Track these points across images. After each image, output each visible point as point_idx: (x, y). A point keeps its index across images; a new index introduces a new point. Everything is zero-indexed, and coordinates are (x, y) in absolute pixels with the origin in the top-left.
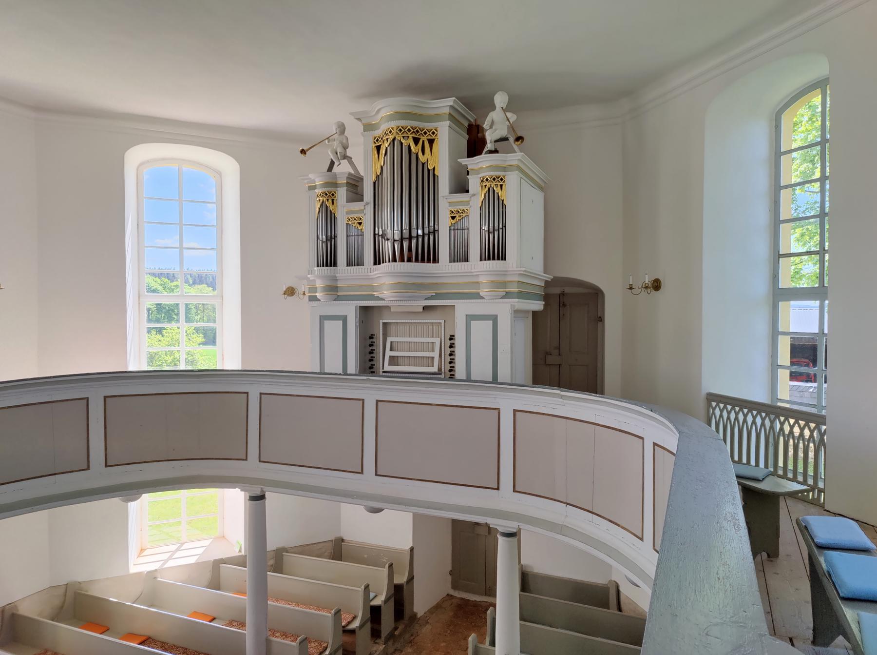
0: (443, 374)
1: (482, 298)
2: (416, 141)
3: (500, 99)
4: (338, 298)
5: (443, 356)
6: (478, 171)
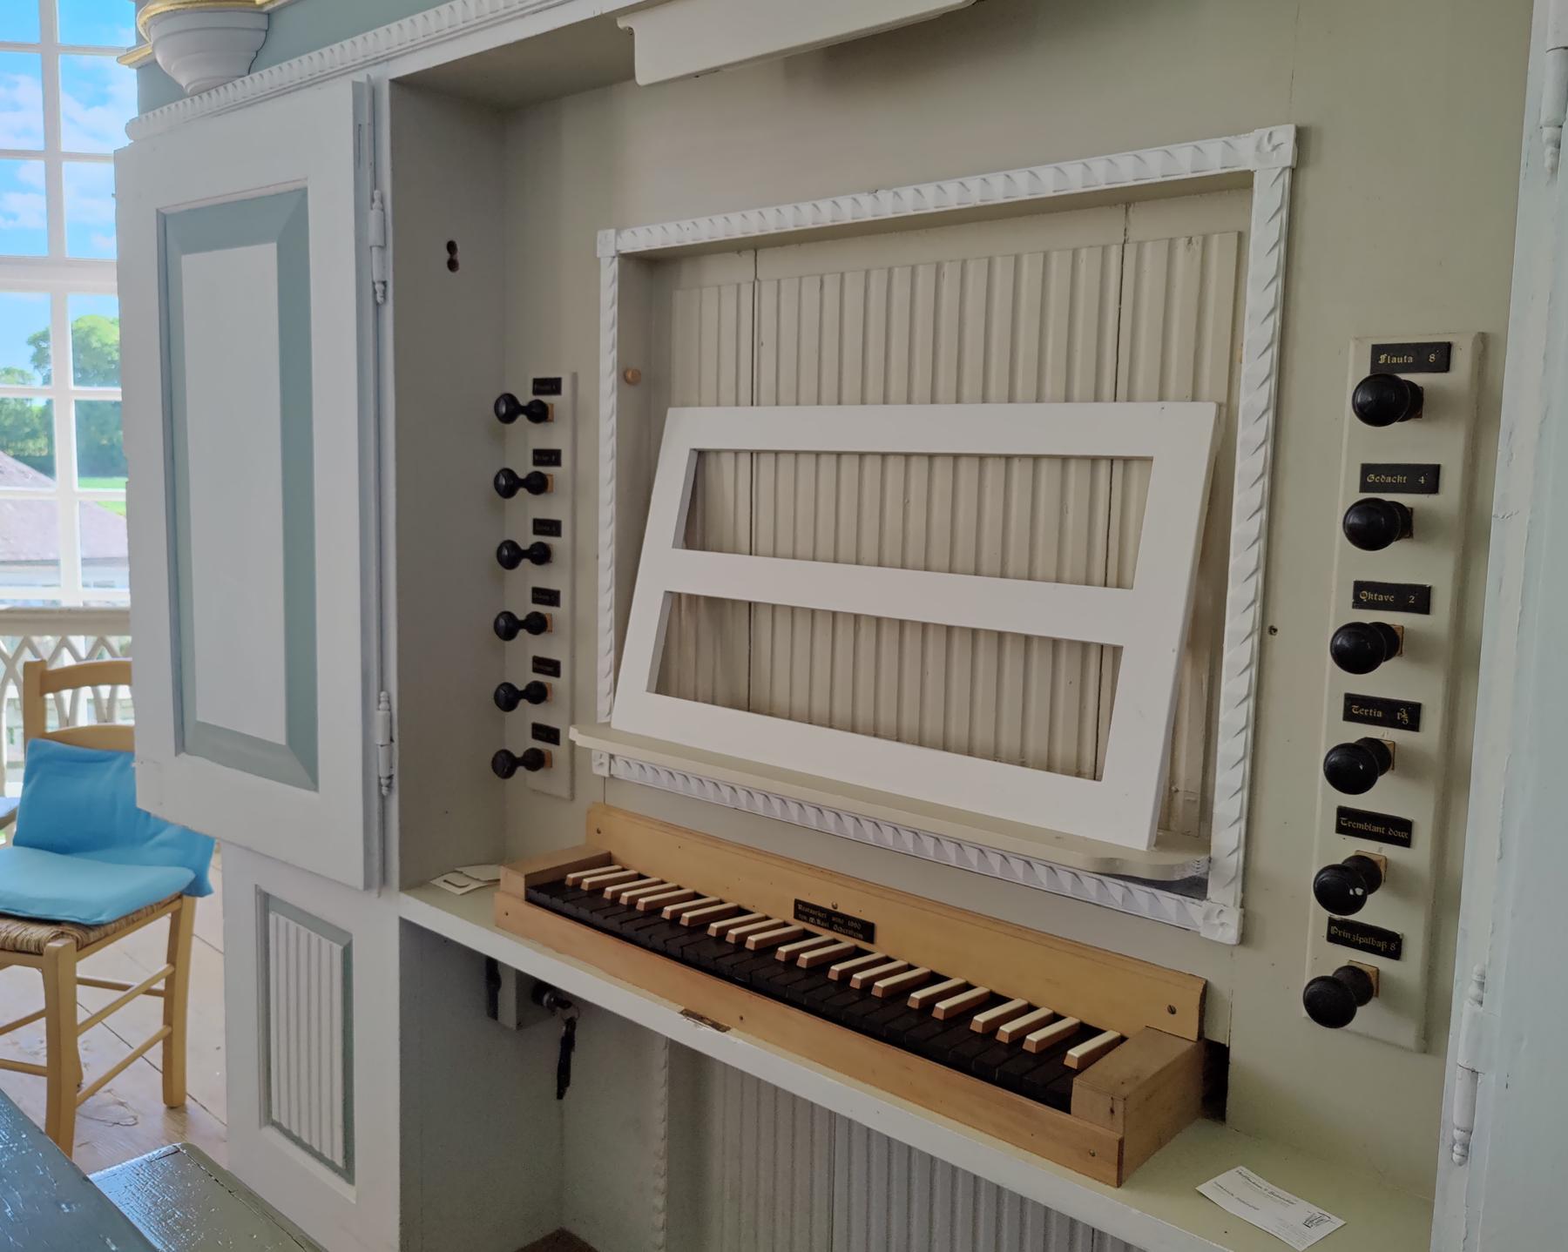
0: (1223, 895)
5: (1237, 651)
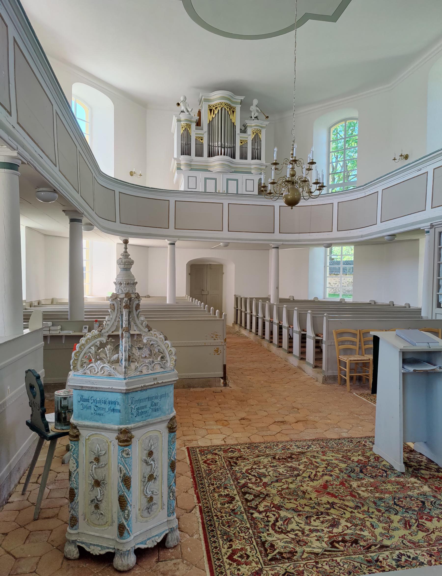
1: (252, 174)
2: (230, 109)
3: (255, 102)
4: (191, 170)
6: (251, 127)
